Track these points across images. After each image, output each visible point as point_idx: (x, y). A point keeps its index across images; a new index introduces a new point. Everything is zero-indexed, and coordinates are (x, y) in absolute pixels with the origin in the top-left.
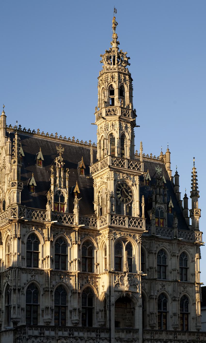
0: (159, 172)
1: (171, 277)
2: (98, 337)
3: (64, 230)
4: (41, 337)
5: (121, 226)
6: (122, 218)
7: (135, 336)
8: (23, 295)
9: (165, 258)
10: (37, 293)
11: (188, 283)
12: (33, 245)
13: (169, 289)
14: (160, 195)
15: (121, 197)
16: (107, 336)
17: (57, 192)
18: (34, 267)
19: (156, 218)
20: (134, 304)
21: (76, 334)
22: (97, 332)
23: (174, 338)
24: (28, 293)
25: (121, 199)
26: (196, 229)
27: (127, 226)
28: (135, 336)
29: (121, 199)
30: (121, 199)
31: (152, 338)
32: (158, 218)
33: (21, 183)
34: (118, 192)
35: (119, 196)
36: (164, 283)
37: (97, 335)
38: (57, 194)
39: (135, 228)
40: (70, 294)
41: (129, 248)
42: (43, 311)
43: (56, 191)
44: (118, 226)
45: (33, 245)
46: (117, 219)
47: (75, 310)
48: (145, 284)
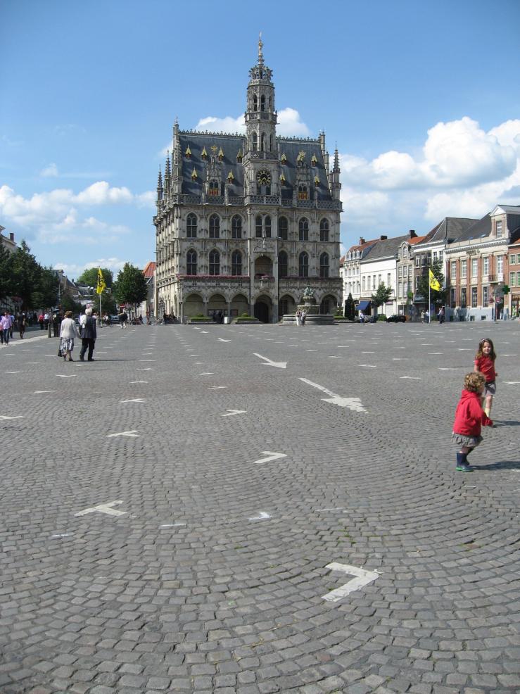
1: (311, 239)
9: (306, 225)
10: (195, 256)
13: (309, 248)
16: (248, 285)
20: (272, 262)
21: (222, 284)
24: (189, 256)
27: (265, 203)
28: (272, 285)
40: (221, 255)
42: (200, 268)
47: (225, 267)
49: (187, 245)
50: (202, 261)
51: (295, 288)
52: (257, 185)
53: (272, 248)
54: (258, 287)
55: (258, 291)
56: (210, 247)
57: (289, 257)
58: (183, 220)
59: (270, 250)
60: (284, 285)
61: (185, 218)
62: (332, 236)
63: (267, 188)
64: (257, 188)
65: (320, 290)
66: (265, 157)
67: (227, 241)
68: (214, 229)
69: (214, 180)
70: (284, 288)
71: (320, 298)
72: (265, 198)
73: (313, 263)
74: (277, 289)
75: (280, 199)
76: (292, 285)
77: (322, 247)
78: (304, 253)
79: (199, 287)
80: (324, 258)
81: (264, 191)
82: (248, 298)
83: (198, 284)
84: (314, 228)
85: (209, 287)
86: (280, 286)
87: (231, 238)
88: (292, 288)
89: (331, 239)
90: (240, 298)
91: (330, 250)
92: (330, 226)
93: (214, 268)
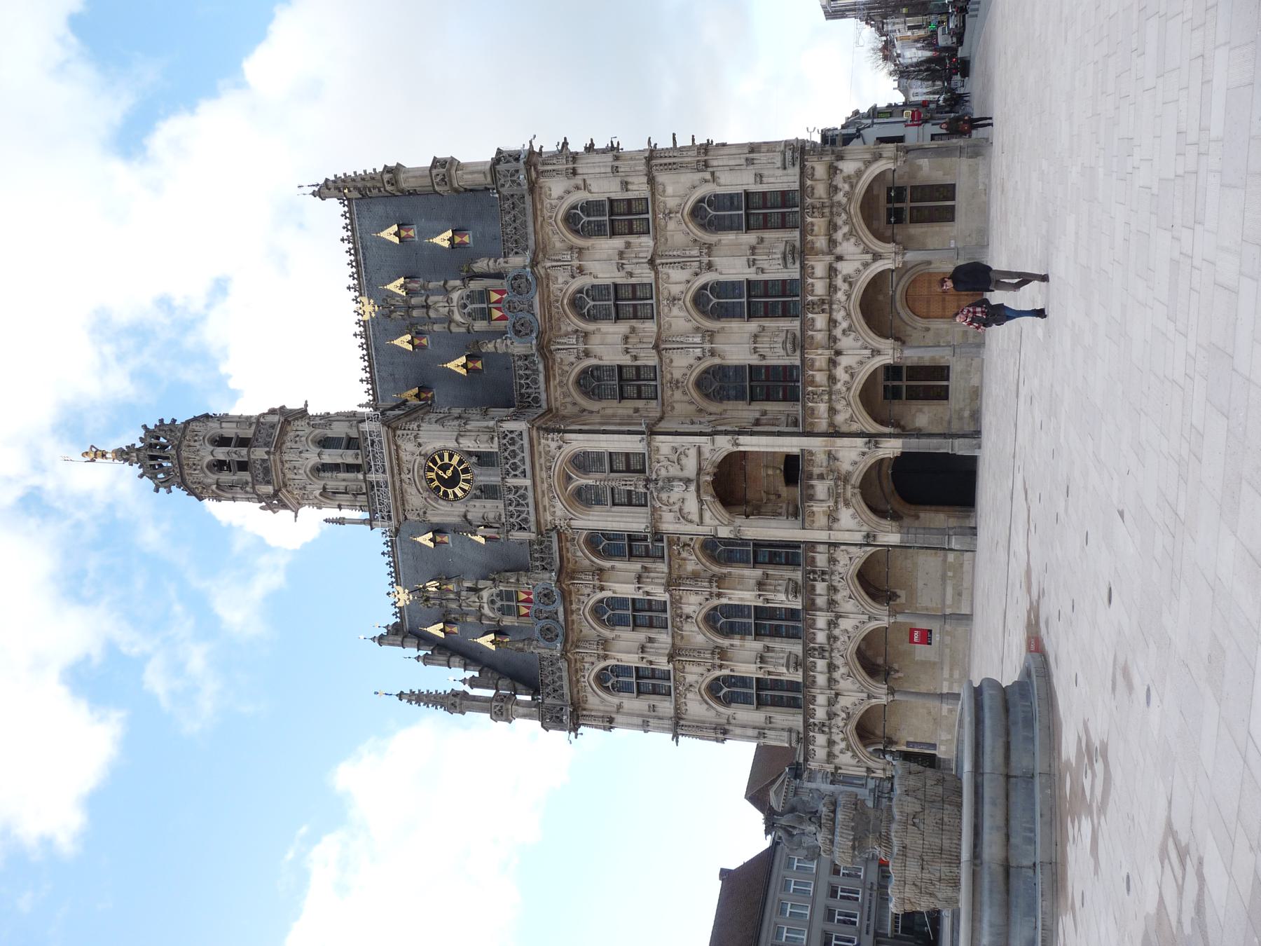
2: (827, 577)
3: (574, 607)
5: (530, 500)
6: (511, 496)
7: (821, 458)
10: (728, 680)
11: (653, 194)
13: (678, 280)
22: (815, 580)
23: (823, 311)
25: (466, 486)
26: (489, 179)
27: (527, 482)
28: (821, 458)
29: (466, 486)
31: (826, 397)
32: (490, 309)
34: (451, 497)
35: (459, 493)
37: (823, 580)
39: (527, 454)
41: (583, 462)
43: (491, 615)
44: (531, 509)
48: (674, 364)
49: (696, 707)
50: (746, 659)
51: (832, 363)
53: (678, 455)
54: (832, 517)
55: (846, 517)
56: (697, 636)
57: (717, 361)
58: (620, 707)
59: (690, 465)
60: (822, 408)
61: (613, 700)
65: (840, 258)
67: (672, 583)
68: (642, 614)
69: (493, 602)
70: (832, 411)
71: (877, 257)
72: (511, 482)
73: (735, 260)
74: (840, 442)
76: (820, 378)
77: (672, 225)
78: (699, 300)
79: (831, 715)
80: (714, 214)
82: (870, 550)
84: (604, 262)
85: (831, 681)
87: (663, 567)
88: (832, 379)
89: (639, 188)
90: (875, 581)
91: (678, 190)
92: (591, 197)
93: (767, 623)
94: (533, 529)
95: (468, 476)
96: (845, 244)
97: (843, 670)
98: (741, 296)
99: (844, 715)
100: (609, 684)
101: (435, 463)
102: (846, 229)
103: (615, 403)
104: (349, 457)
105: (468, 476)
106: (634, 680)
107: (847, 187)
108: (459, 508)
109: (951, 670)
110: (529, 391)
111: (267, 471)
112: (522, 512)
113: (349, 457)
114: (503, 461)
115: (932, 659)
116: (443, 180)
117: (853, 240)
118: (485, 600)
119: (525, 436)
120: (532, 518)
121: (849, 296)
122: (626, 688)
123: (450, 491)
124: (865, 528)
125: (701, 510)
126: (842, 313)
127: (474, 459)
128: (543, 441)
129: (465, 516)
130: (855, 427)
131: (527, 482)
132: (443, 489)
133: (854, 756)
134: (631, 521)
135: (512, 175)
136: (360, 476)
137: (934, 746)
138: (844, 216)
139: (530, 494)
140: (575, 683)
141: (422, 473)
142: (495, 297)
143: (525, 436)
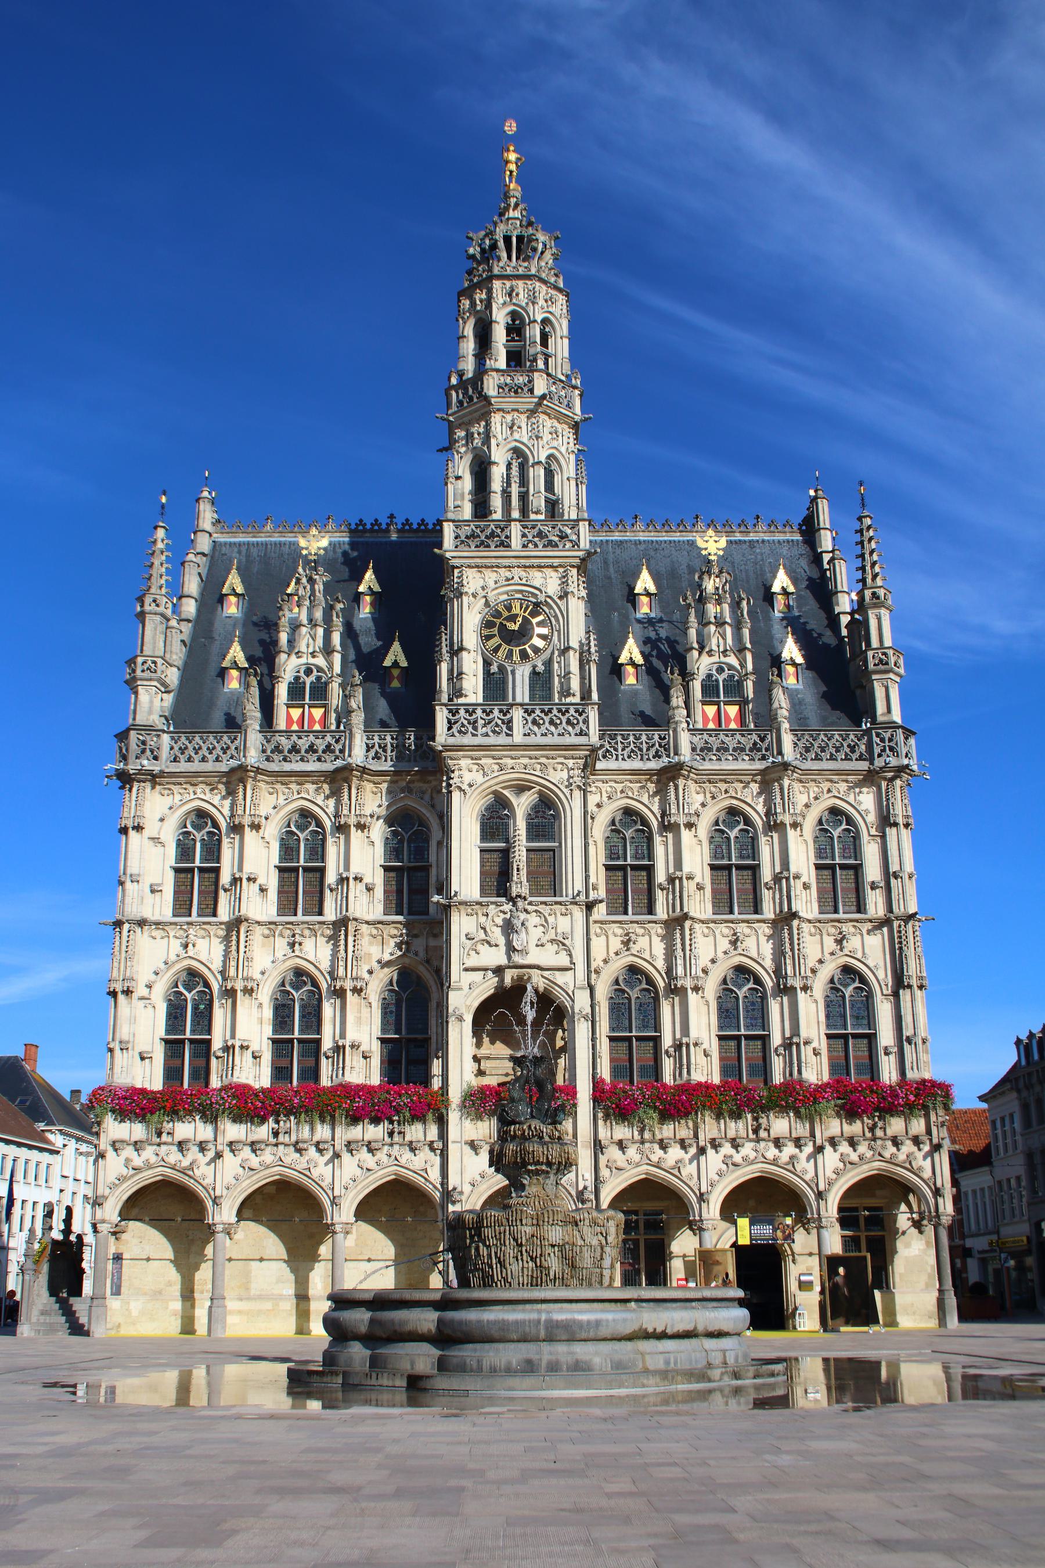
0: (713, 550)
3: (311, 787)
4: (159, 1145)
5: (492, 740)
6: (496, 712)
8: (150, 1009)
12: (198, 845)
14: (720, 623)
15: (500, 646)
17: (298, 672)
18: (199, 915)
19: (704, 703)
30: (500, 654)
32: (718, 704)
33: (155, 662)
36: (742, 929)
38: (297, 678)
44: (479, 740)
45: (198, 845)
46: (476, 722)
52: (487, 663)
53: (561, 943)
59: (548, 956)
62: (874, 886)
63: (534, 673)
64: (487, 674)
66: (516, 541)
72: (517, 714)
75: (593, 715)
81: (521, 689)
83: (184, 1129)
86: (603, 1133)
94: (451, 741)
95: (516, 657)
96: (837, 1155)
97: (254, 1161)
98: (747, 1028)
99: (186, 1163)
100: (190, 829)
101: (534, 614)
102: (854, 1157)
103: (602, 860)
104: (538, 501)
105: (516, 657)
106: (197, 863)
107: (902, 1157)
108: (471, 638)
109: (240, 1312)
110: (620, 747)
111: (516, 390)
112: (475, 728)
113: (538, 501)
114: (546, 708)
115: (253, 1286)
116: (881, 660)
117: (841, 1165)
118: (311, 661)
119: (582, 740)
120: (468, 740)
121: (775, 1162)
122: (185, 850)
123: (495, 631)
124: (467, 1188)
125: (486, 970)
126: (752, 1155)
127: (540, 668)
128: (570, 763)
129: (461, 649)
130: (604, 1172)
131: (518, 738)
132: (498, 621)
133: (122, 1179)
134: (466, 871)
135: (891, 749)
136: (515, 514)
137: (117, 1291)
138: (869, 1154)
139: (502, 740)
140: (192, 778)
141: (520, 596)
142: (733, 710)
143: (582, 740)
